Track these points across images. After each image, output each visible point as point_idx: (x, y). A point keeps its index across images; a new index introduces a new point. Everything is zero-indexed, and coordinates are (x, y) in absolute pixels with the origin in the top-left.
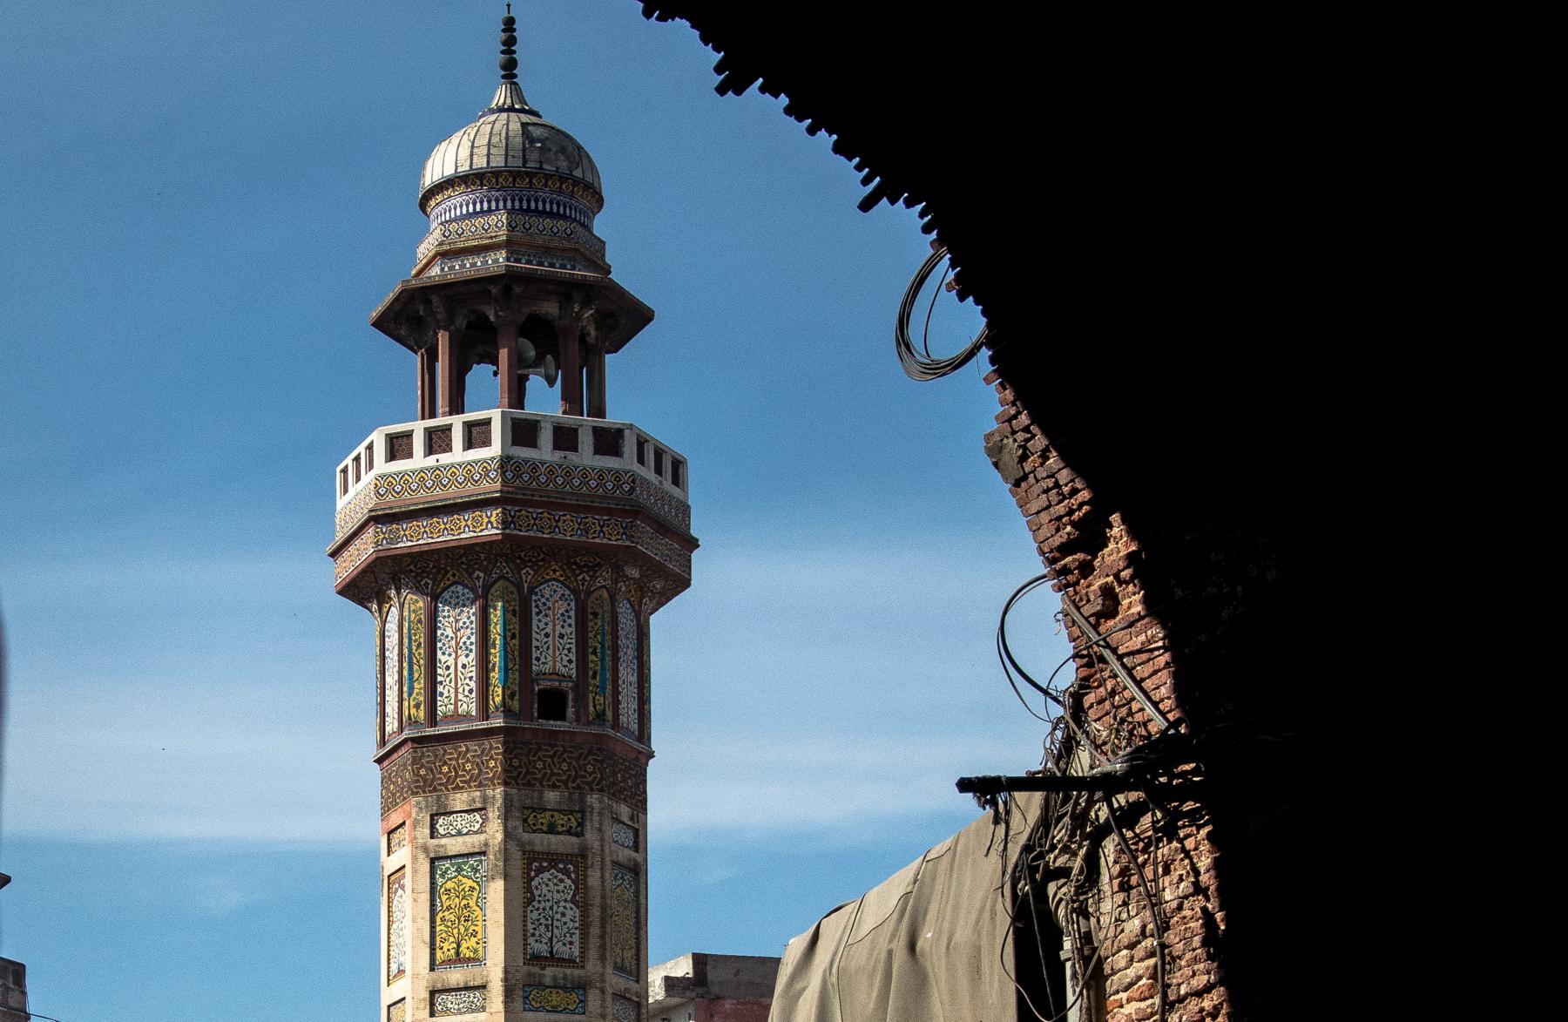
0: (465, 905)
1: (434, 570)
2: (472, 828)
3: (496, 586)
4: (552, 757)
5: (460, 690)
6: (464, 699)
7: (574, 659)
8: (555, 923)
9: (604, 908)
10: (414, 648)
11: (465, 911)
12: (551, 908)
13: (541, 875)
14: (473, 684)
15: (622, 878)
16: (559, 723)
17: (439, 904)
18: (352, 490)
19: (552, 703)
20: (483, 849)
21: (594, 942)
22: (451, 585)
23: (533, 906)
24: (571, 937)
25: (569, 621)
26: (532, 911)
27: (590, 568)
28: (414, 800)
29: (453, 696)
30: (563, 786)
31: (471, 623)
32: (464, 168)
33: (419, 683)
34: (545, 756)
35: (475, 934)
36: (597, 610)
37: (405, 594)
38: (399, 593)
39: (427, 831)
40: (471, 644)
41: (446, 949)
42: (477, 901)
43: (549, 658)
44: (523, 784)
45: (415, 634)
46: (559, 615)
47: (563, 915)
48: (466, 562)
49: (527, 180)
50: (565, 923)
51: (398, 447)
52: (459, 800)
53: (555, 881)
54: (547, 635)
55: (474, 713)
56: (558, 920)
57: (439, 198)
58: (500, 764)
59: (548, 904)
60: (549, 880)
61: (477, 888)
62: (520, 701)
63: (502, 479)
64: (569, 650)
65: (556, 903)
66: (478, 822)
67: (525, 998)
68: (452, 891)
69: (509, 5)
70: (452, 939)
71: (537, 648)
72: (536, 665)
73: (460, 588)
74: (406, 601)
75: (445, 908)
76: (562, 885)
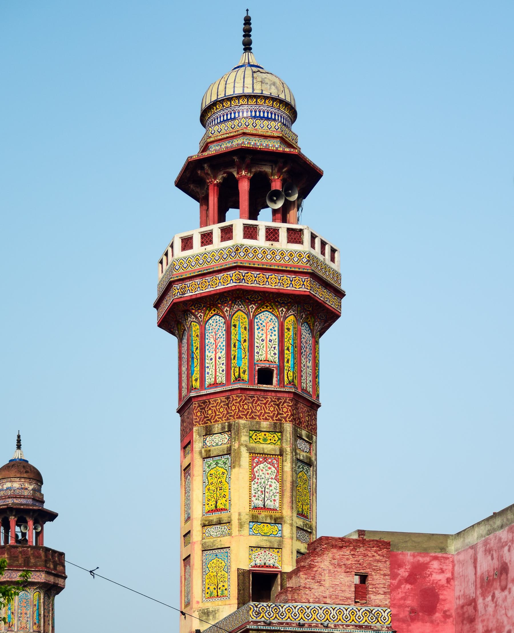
2: (224, 442)
4: (265, 404)
5: (218, 370)
6: (220, 375)
8: (266, 490)
11: (220, 485)
12: (264, 483)
13: (259, 465)
15: (303, 468)
16: (269, 386)
17: (207, 482)
23: (255, 482)
25: (274, 333)
26: (254, 484)
29: (214, 374)
30: (271, 419)
31: (223, 335)
34: (261, 404)
35: (224, 496)
36: (289, 327)
40: (223, 346)
44: (250, 418)
46: (269, 330)
47: (271, 486)
48: (220, 302)
50: (271, 490)
53: (266, 468)
54: (263, 340)
55: (224, 382)
56: (268, 488)
59: (263, 480)
60: (263, 468)
61: (226, 472)
64: (274, 348)
65: (267, 480)
67: (251, 528)
68: (214, 475)
69: (247, 10)
70: (213, 499)
71: (257, 347)
73: (218, 317)
75: (210, 484)
76: (270, 470)
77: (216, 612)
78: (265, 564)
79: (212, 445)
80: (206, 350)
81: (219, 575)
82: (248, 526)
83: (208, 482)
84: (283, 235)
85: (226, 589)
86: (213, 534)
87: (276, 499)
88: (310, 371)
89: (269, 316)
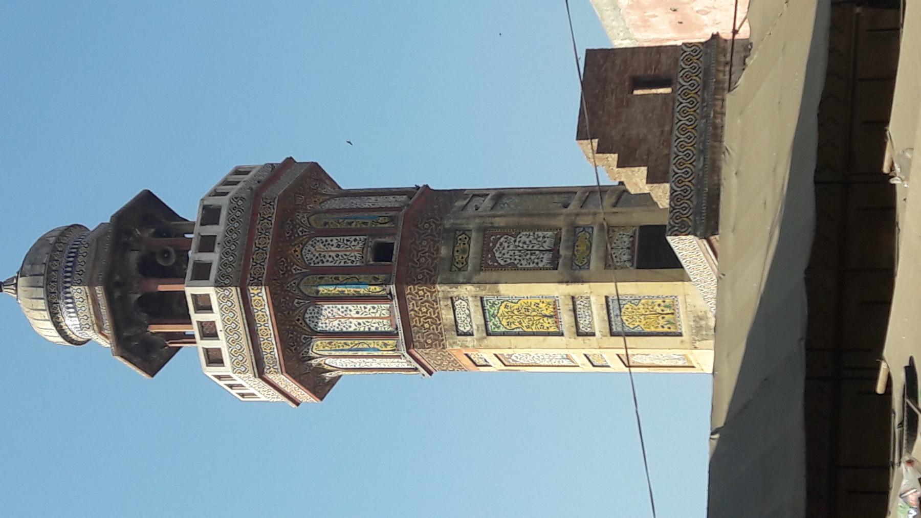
0: (518, 312)
1: (295, 333)
2: (465, 307)
5: (373, 315)
7: (354, 238)
8: (530, 248)
9: (521, 215)
10: (348, 347)
11: (521, 312)
12: (520, 251)
13: (497, 259)
14: (369, 306)
16: (395, 247)
18: (251, 391)
19: (383, 253)
20: (479, 298)
21: (544, 222)
22: (306, 323)
23: (518, 263)
24: (540, 237)
26: (521, 265)
28: (449, 348)
29: (377, 320)
30: (438, 244)
31: (329, 308)
32: (46, 315)
33: (371, 344)
37: (313, 354)
38: (314, 358)
39: (469, 338)
40: (342, 308)
41: (551, 327)
42: (515, 303)
43: (352, 254)
44: (435, 271)
45: (339, 346)
49: (53, 273)
51: (214, 358)
52: (447, 316)
56: (528, 247)
57: (69, 332)
58: (421, 287)
59: (517, 253)
60: (501, 253)
61: (505, 303)
62: (378, 274)
63: (230, 286)
65: (516, 248)
66: (461, 303)
67: (580, 268)
68: (508, 320)
70: (541, 321)
71: (345, 262)
72: (356, 264)
73: (307, 316)
74: (318, 352)
75: (520, 326)
76: (504, 244)
78: (628, 248)
79: (470, 323)
80: (347, 331)
81: (643, 312)
82: (577, 272)
83: (519, 328)
84: (210, 230)
85: (664, 302)
86: (587, 320)
87: (542, 235)
88: (380, 199)
89: (308, 248)
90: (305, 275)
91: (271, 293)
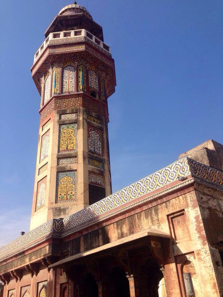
1: (64, 61)
3: (81, 66)
7: (98, 87)
10: (57, 78)
14: (74, 85)
20: (76, 122)
22: (67, 66)
27: (102, 71)
35: (73, 143)
42: (74, 135)
47: (97, 143)
50: (98, 145)
59: (94, 139)
70: (65, 145)
75: (63, 137)
77: (66, 209)
81: (68, 186)
90: (86, 67)
91: (82, 52)
